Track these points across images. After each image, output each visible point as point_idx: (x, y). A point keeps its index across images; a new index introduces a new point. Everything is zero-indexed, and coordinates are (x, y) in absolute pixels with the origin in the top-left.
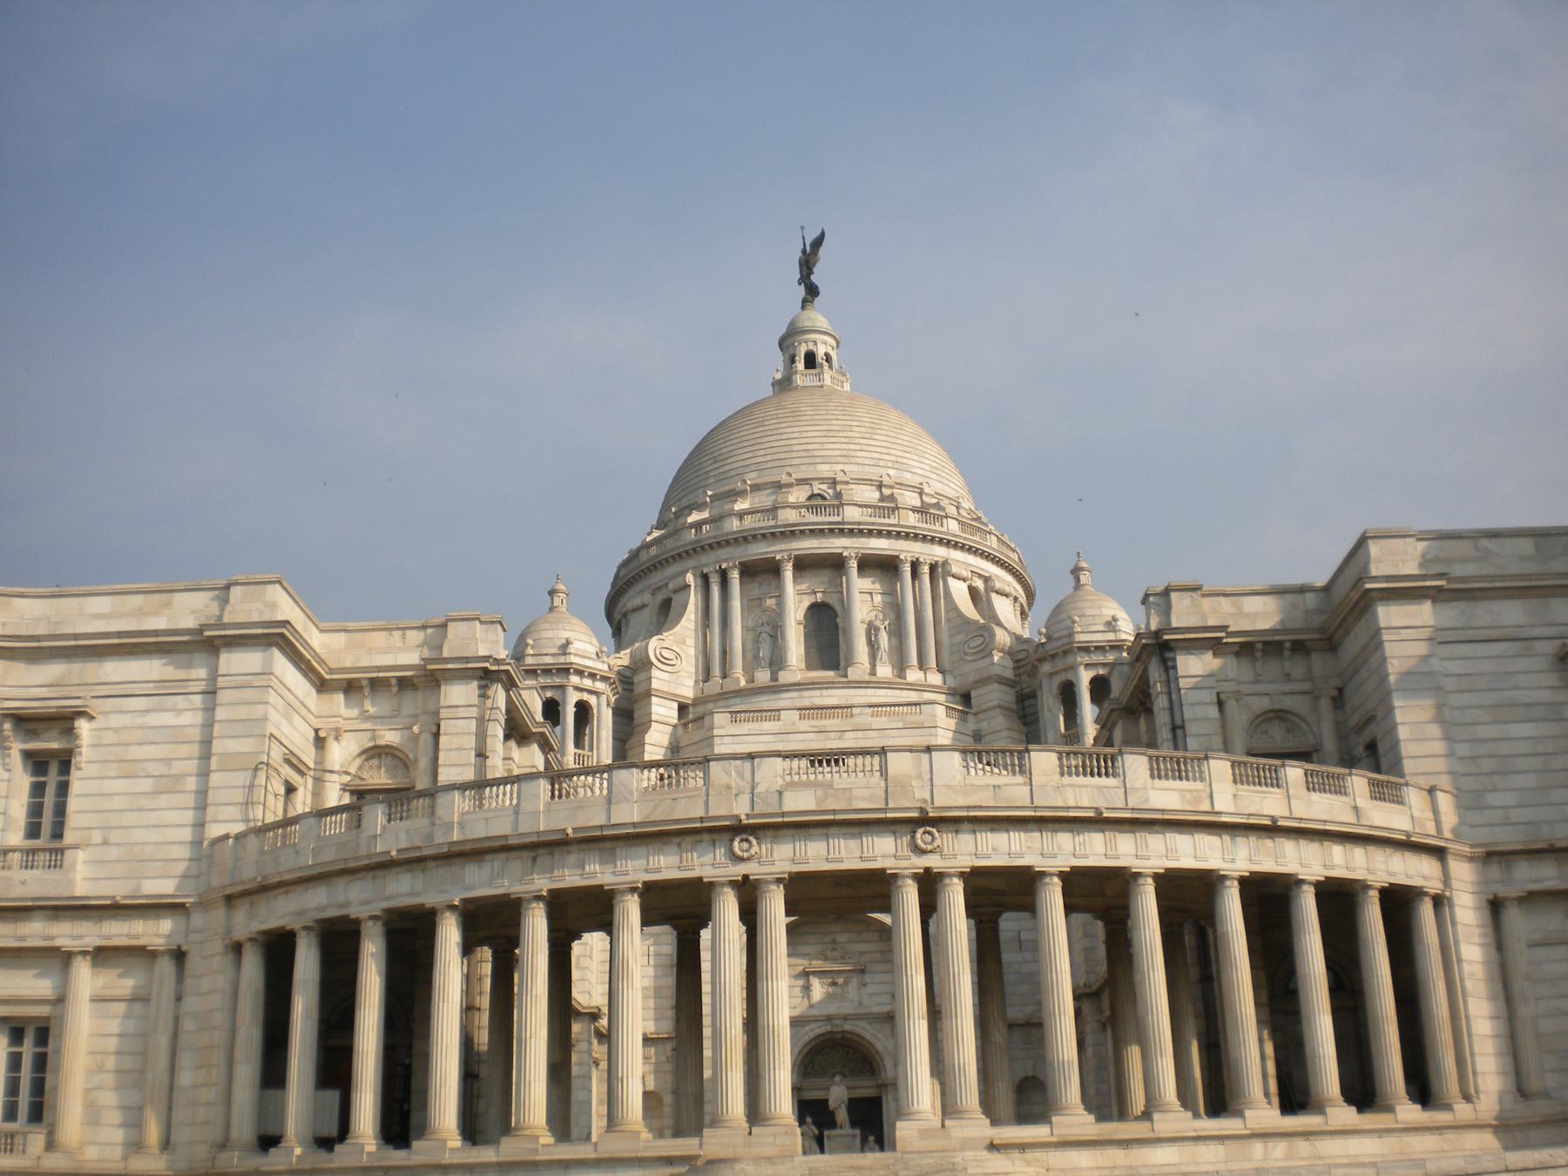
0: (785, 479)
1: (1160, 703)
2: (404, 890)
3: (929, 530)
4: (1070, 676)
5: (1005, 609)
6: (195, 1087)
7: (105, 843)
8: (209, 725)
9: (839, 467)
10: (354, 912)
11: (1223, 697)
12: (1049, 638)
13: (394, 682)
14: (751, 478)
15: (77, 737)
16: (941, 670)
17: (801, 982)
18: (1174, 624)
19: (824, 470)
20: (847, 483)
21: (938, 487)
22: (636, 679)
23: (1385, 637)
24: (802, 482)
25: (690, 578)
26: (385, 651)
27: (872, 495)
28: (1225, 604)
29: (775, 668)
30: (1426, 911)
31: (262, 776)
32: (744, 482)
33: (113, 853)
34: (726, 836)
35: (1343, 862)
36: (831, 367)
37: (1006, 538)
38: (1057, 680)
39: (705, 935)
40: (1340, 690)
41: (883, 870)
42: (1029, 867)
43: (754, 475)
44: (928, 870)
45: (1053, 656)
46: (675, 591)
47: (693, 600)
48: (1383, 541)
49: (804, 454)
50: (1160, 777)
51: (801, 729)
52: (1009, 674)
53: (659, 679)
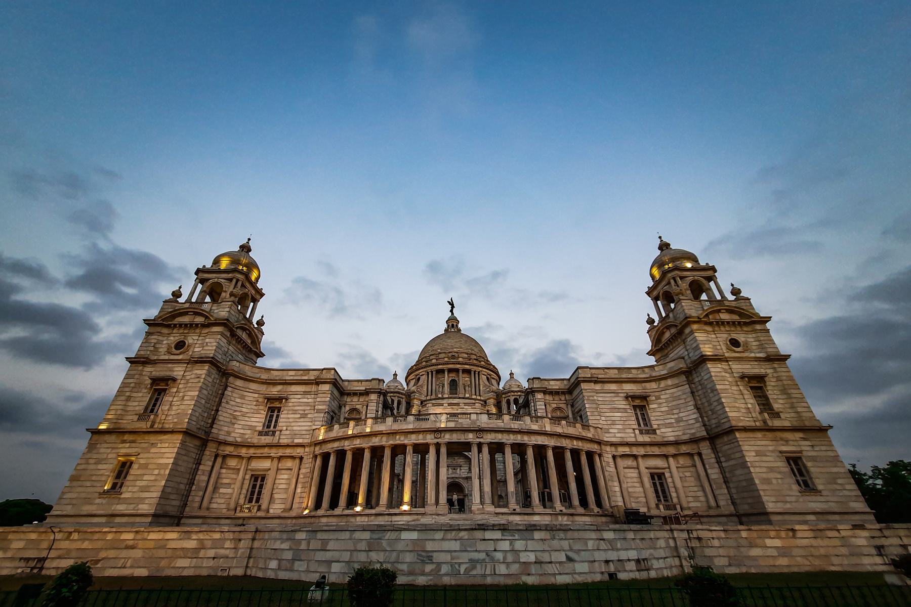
4: (509, 398)
5: (494, 382)
6: (301, 493)
7: (287, 430)
10: (346, 448)
16: (480, 396)
18: (535, 386)
19: (455, 350)
24: (451, 352)
28: (546, 383)
33: (288, 432)
35: (576, 444)
38: (506, 399)
39: (427, 456)
40: (573, 403)
41: (470, 442)
44: (480, 442)
45: (506, 393)
46: (421, 376)
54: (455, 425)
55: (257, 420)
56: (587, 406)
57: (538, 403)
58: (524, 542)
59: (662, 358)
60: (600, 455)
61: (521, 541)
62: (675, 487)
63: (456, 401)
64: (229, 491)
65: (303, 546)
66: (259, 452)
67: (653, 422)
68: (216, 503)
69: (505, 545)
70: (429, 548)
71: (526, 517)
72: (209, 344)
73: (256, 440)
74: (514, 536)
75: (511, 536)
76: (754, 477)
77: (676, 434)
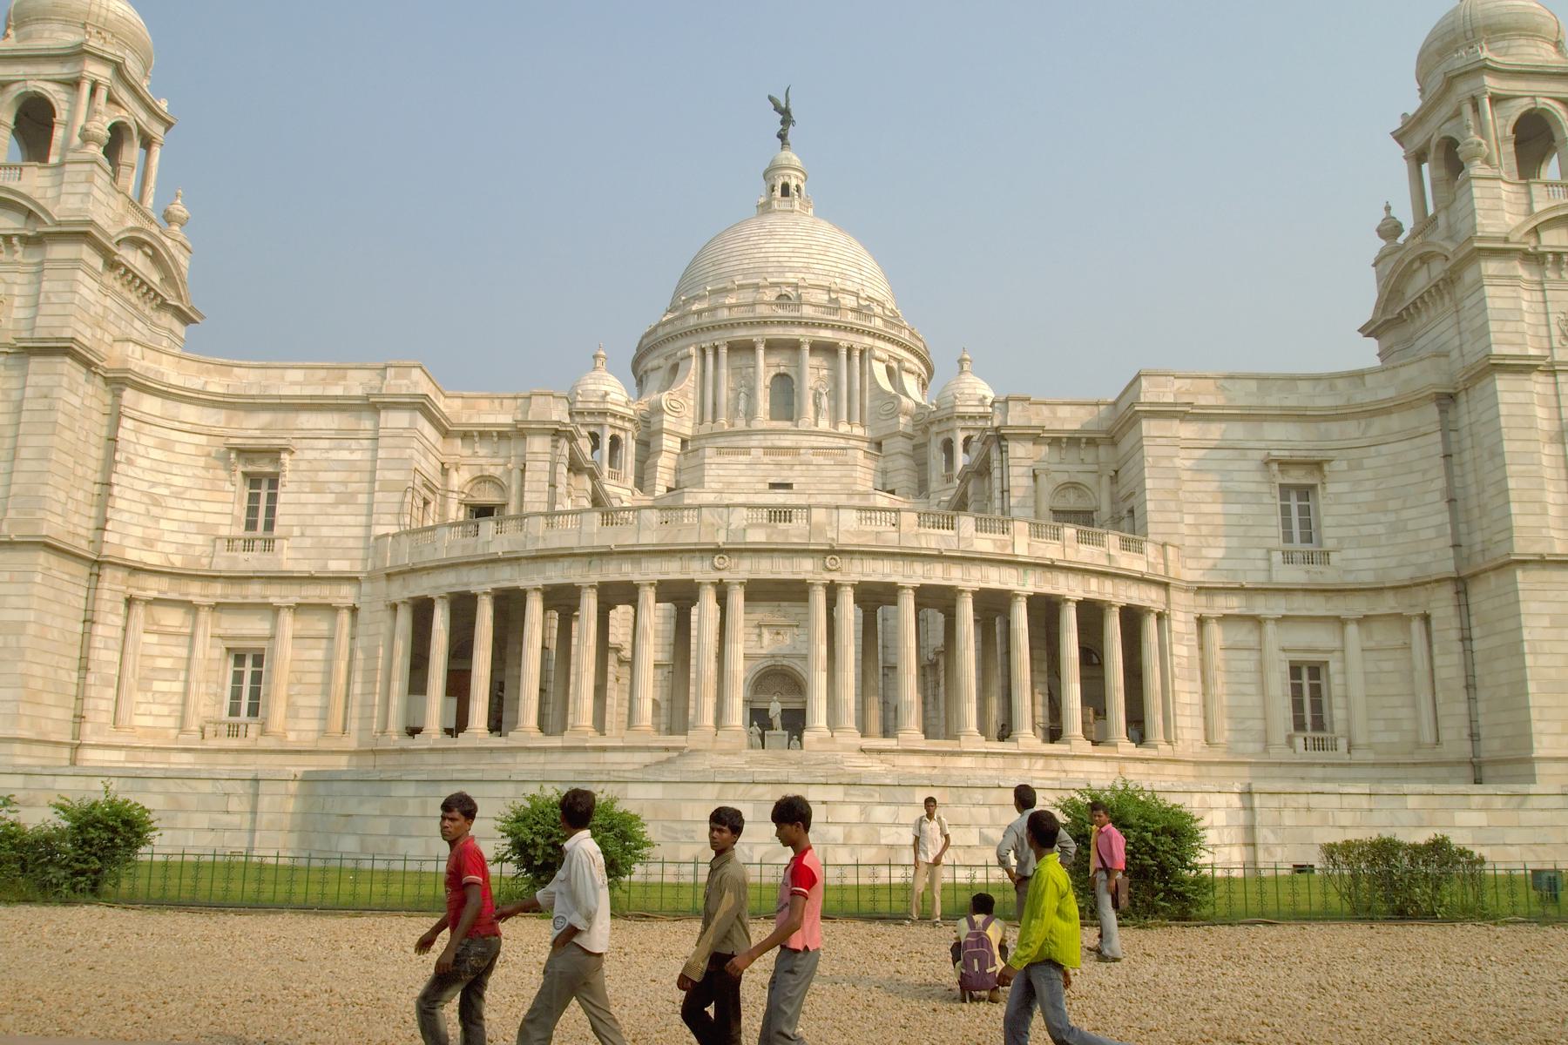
0: (762, 282)
1: (996, 473)
2: (507, 578)
3: (862, 325)
4: (950, 435)
5: (910, 383)
7: (303, 535)
8: (374, 460)
10: (473, 589)
12: (938, 408)
13: (495, 434)
14: (739, 280)
15: (282, 465)
16: (862, 425)
17: (757, 631)
18: (1009, 424)
19: (791, 277)
20: (806, 288)
21: (871, 293)
22: (652, 420)
23: (1144, 443)
25: (692, 350)
27: (823, 297)
28: (1045, 410)
29: (748, 417)
30: (1151, 625)
31: (409, 496)
32: (734, 282)
33: (308, 542)
34: (710, 555)
35: (1095, 589)
36: (800, 196)
39: (694, 610)
40: (1116, 472)
42: (895, 583)
44: (832, 581)
48: (1152, 378)
49: (775, 264)
50: (981, 531)
52: (909, 430)
53: (668, 422)
54: (769, 536)
55: (217, 507)
56: (1149, 484)
57: (1014, 471)
58: (893, 808)
59: (1395, 348)
61: (886, 808)
63: (787, 441)
66: (234, 594)
68: (150, 714)
69: (851, 813)
70: (686, 816)
71: (938, 760)
72: (54, 299)
73: (222, 564)
74: (871, 796)
75: (865, 795)
76: (1529, 677)
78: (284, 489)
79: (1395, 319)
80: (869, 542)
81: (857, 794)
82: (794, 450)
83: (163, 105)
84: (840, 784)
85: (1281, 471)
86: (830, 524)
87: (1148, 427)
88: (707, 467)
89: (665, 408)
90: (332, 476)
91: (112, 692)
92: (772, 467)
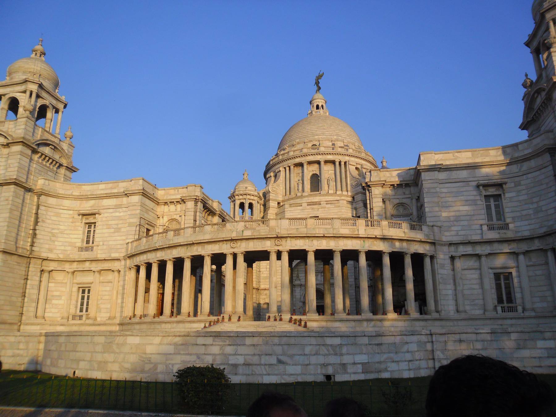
2: (161, 255)
9: (321, 136)
11: (384, 200)
25: (281, 169)
26: (174, 195)
33: (105, 247)
34: (229, 242)
37: (368, 153)
40: (419, 197)
41: (266, 251)
43: (298, 140)
44: (278, 250)
46: (278, 172)
47: (282, 174)
49: (311, 134)
51: (308, 208)
53: (272, 196)
57: (375, 200)
58: (235, 347)
59: (534, 133)
60: (432, 257)
61: (232, 347)
62: (521, 287)
63: (316, 199)
64: (61, 302)
65: (63, 348)
66: (81, 267)
67: (507, 215)
74: (225, 342)
75: (222, 341)
77: (532, 227)
78: (98, 228)
79: (531, 120)
80: (294, 233)
81: (219, 342)
82: (319, 203)
83: (63, 98)
84: (211, 336)
85: (485, 190)
86: (278, 226)
87: (424, 176)
88: (286, 212)
89: (270, 191)
90: (113, 222)
91: (34, 305)
92: (310, 210)
